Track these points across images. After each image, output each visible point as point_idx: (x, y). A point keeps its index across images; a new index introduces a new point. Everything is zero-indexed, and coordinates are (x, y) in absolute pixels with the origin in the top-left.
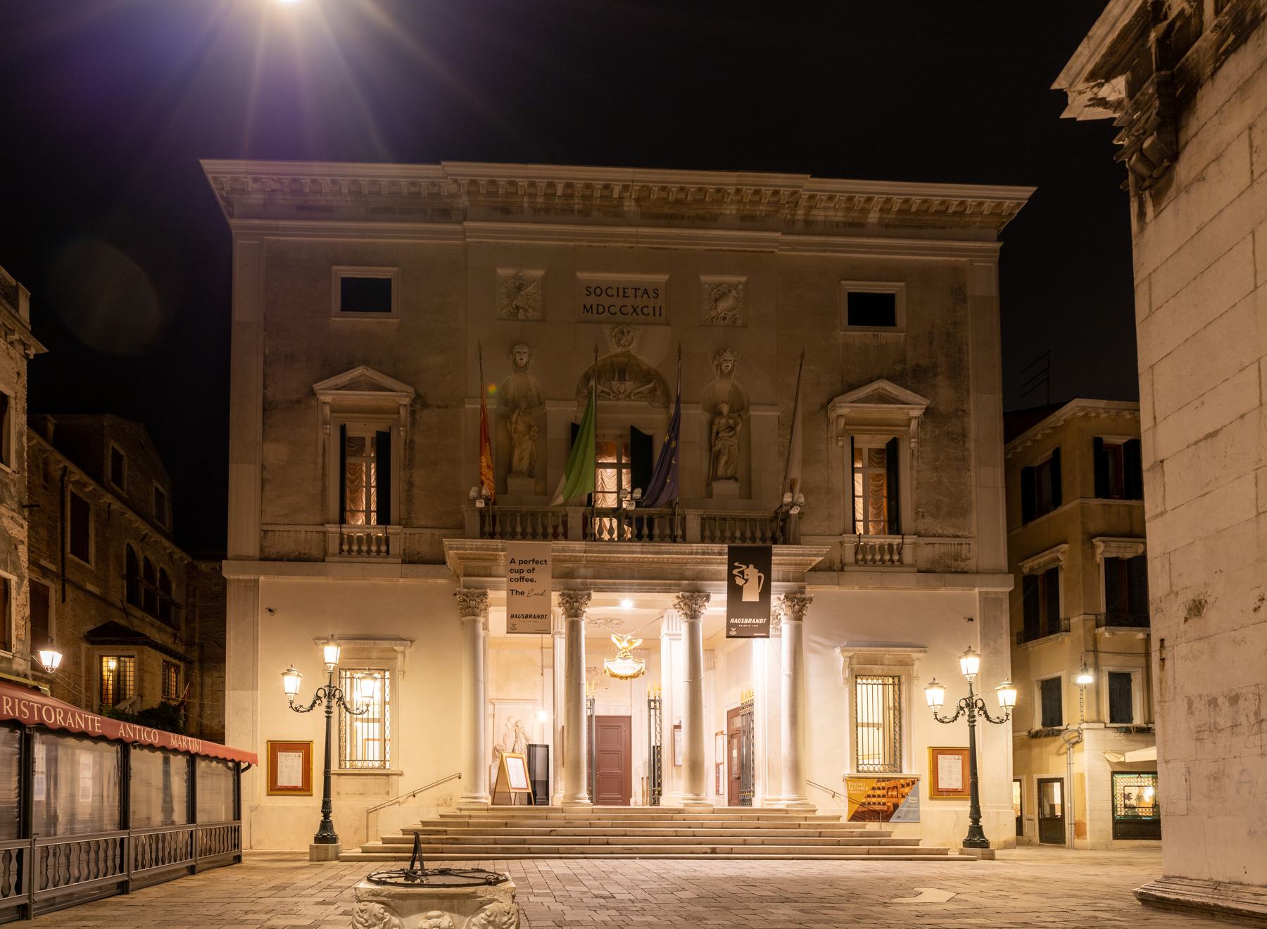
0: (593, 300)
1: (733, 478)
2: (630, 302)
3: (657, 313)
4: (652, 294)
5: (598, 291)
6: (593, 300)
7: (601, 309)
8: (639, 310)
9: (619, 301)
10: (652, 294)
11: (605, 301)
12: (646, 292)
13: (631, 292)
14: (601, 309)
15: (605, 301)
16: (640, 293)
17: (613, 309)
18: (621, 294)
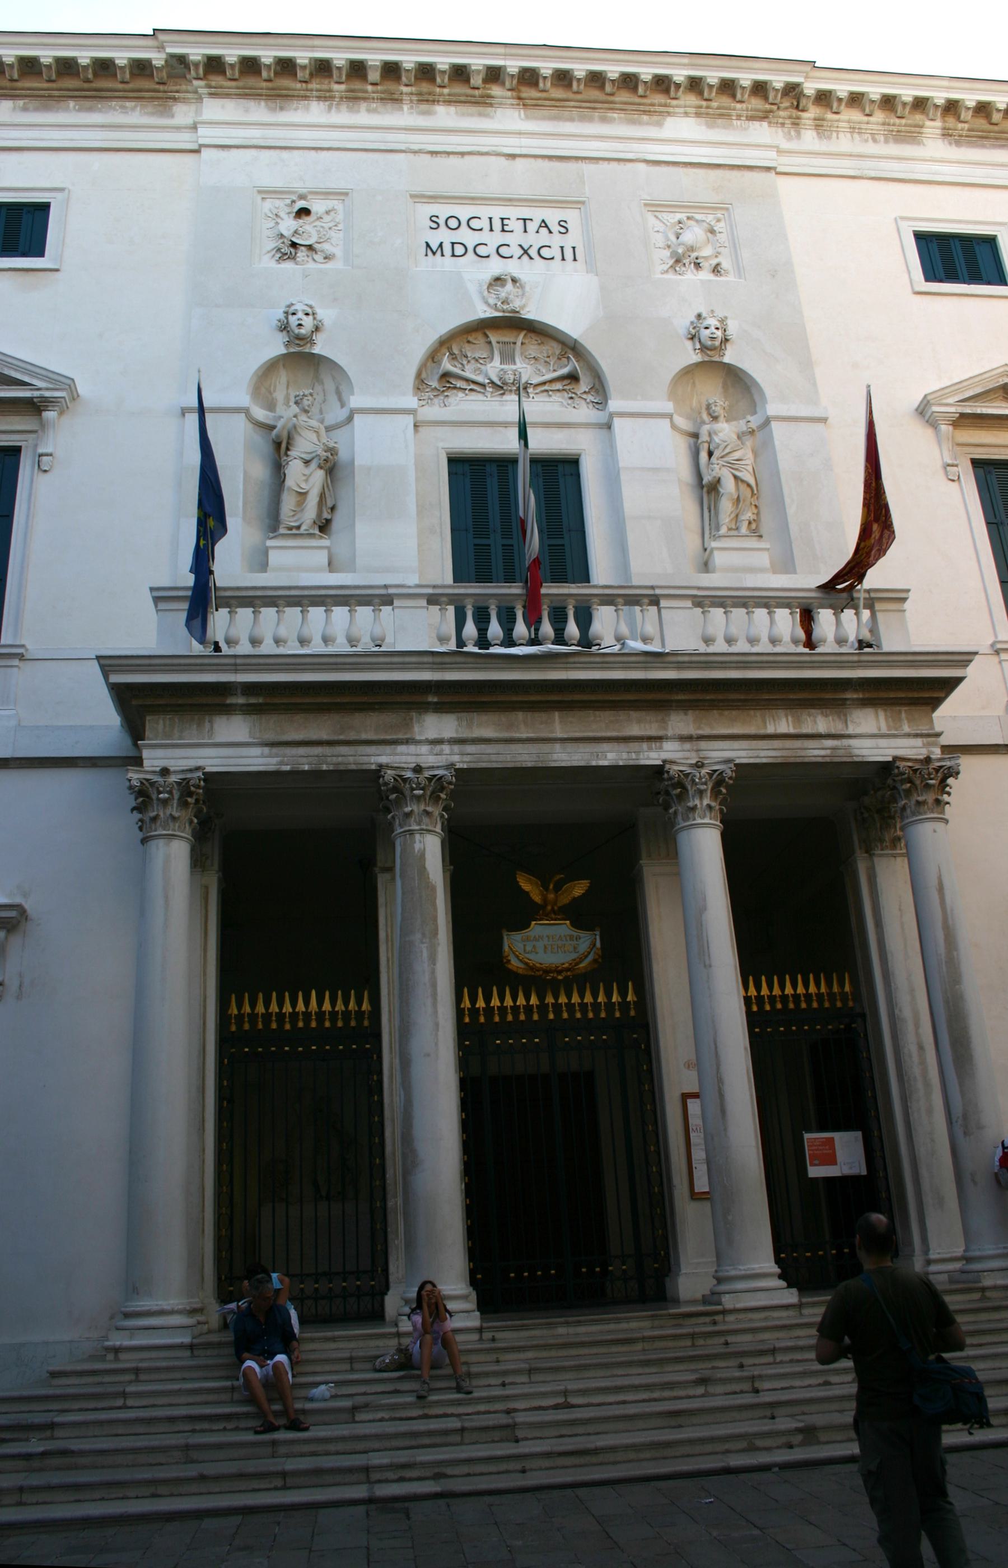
0: (444, 236)
1: (755, 531)
2: (515, 239)
3: (569, 254)
4: (555, 228)
5: (453, 223)
6: (444, 236)
7: (459, 250)
8: (533, 252)
9: (497, 238)
10: (555, 228)
11: (465, 236)
12: (544, 224)
13: (517, 226)
14: (459, 250)
15: (465, 236)
16: (532, 227)
17: (481, 250)
18: (497, 225)
